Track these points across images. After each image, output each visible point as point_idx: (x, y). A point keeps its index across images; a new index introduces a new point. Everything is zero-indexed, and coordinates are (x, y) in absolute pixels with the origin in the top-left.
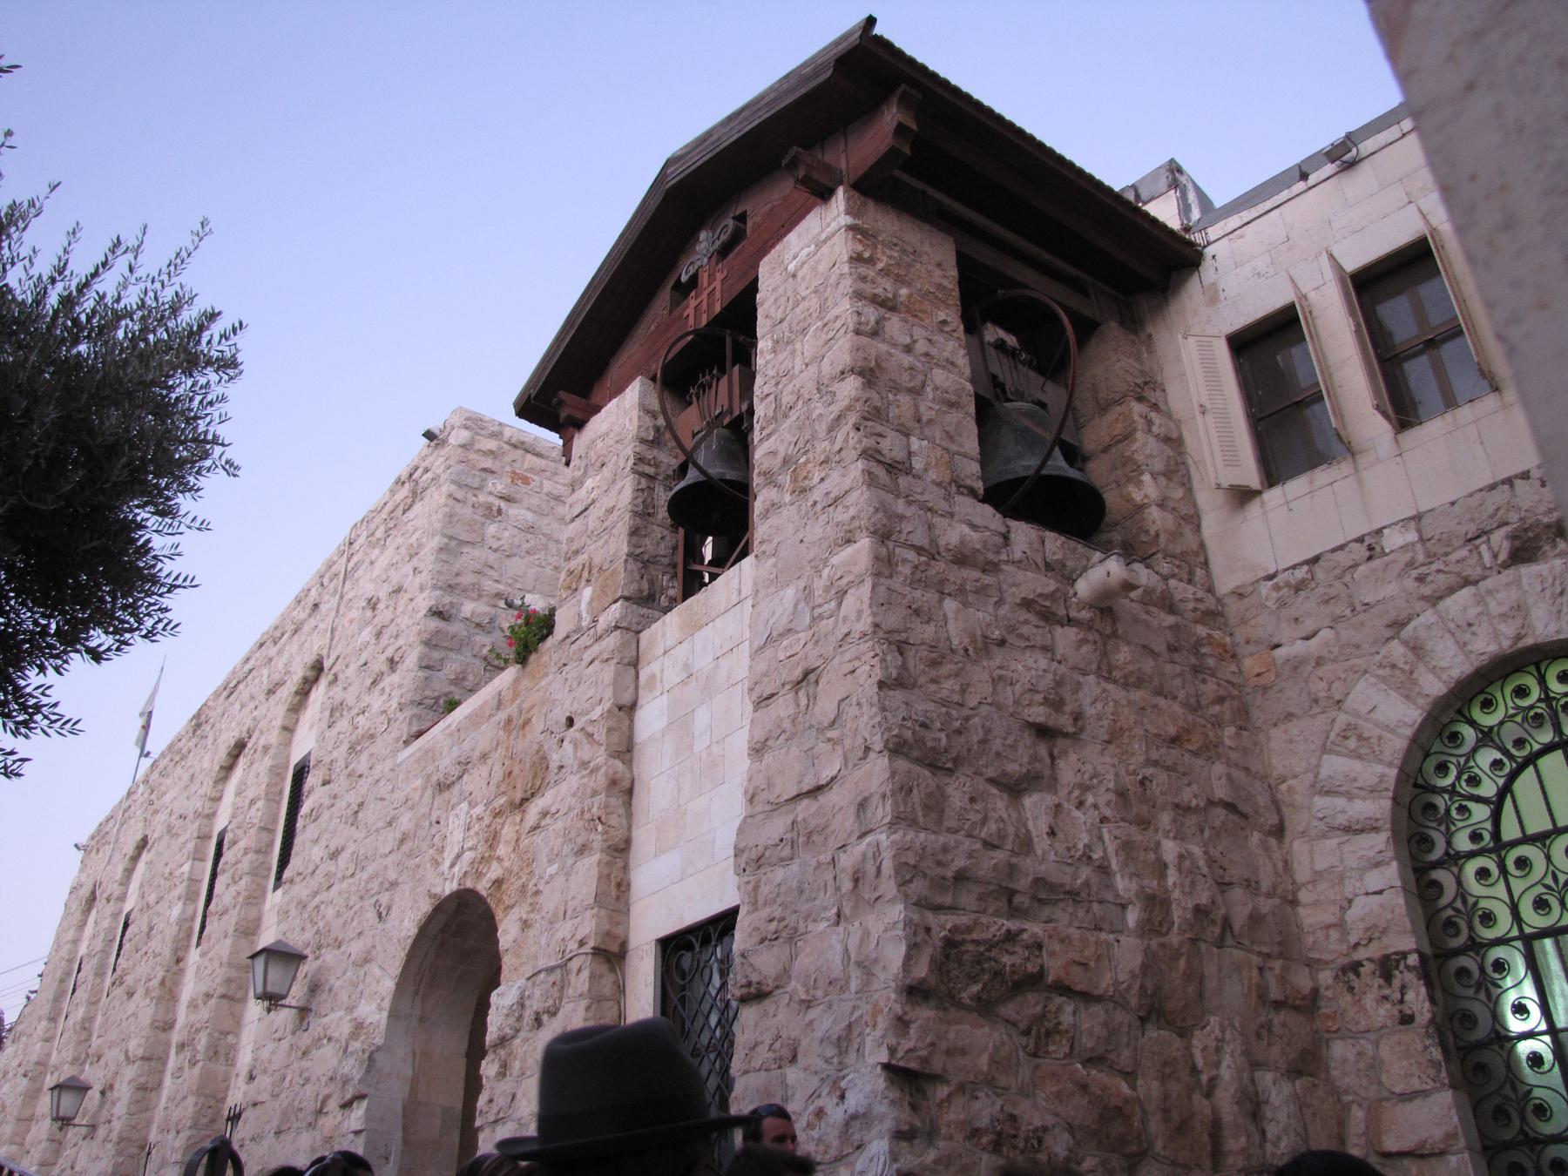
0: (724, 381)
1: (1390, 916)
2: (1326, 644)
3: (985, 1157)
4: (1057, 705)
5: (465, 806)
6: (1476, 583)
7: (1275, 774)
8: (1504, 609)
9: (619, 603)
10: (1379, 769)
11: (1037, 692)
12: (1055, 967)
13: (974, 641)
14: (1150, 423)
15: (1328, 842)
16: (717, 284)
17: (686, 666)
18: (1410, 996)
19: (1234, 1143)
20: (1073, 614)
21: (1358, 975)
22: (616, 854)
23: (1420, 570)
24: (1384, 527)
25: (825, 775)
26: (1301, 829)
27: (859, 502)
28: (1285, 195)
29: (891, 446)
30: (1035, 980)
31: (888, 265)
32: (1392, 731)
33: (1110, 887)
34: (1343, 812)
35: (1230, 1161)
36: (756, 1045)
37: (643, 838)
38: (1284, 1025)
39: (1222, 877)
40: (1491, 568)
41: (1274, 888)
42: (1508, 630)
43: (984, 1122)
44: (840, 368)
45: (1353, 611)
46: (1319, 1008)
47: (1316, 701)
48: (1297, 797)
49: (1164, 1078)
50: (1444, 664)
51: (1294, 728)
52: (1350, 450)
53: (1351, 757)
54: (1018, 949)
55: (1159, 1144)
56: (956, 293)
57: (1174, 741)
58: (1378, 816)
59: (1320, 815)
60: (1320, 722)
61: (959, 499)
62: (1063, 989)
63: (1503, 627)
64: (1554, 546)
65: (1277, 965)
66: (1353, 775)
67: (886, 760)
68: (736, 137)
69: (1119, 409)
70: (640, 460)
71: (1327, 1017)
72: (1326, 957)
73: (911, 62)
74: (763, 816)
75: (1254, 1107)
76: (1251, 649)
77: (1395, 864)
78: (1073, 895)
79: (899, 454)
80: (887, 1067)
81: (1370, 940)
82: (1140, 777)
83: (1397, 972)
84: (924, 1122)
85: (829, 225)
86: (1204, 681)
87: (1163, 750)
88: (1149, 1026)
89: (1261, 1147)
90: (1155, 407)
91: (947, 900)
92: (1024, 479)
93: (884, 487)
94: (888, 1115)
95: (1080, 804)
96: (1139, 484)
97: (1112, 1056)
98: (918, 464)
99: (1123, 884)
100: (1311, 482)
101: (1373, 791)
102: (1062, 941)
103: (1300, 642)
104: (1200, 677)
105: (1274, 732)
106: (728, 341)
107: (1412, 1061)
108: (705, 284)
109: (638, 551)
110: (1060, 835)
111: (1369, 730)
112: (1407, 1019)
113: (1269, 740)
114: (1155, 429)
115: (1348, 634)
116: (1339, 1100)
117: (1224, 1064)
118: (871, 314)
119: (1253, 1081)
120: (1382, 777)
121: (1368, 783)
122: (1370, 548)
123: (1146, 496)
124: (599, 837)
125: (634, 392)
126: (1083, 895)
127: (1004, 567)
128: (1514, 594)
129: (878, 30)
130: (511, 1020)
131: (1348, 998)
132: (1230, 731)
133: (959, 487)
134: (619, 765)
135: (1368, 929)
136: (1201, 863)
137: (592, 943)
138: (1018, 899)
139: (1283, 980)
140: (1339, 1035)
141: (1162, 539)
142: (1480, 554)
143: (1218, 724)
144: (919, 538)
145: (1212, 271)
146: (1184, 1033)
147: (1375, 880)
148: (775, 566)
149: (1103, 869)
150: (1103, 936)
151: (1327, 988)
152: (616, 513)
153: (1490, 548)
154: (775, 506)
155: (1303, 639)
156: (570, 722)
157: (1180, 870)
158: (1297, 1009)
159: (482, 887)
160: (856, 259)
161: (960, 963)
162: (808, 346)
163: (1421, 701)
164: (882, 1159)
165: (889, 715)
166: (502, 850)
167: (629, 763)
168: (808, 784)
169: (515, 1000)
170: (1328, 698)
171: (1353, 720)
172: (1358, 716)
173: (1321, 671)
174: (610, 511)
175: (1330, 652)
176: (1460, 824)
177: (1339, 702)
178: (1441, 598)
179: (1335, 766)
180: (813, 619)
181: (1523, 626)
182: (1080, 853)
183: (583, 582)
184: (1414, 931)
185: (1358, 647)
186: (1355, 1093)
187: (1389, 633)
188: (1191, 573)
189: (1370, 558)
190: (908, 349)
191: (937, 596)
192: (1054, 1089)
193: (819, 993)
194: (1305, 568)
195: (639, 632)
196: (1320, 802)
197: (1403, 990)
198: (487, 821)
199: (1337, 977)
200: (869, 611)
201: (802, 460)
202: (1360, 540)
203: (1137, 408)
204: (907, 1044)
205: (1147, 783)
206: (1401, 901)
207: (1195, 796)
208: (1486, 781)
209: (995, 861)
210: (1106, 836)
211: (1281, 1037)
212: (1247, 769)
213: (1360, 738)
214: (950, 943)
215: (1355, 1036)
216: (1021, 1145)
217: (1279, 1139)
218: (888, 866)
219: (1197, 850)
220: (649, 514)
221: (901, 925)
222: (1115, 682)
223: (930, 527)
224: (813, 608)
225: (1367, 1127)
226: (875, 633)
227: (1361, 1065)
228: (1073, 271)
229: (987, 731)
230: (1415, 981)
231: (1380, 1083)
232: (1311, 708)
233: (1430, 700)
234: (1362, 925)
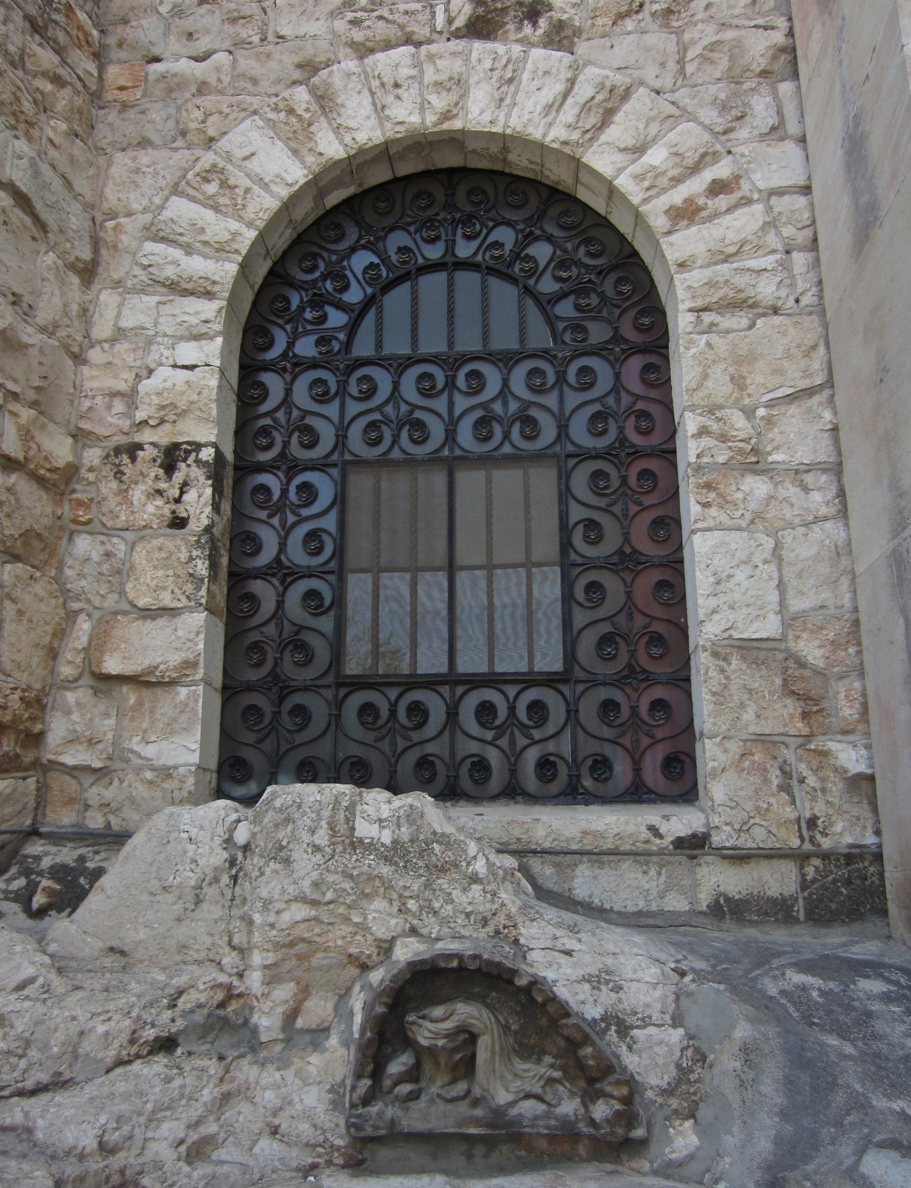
1: (195, 397)
2: (218, 69)
6: (418, 44)
7: (105, 206)
8: (442, 77)
10: (235, 225)
15: (145, 298)
18: (190, 496)
21: (133, 459)
23: (359, 14)
26: (116, 276)
32: (265, 186)
34: (176, 263)
40: (440, 33)
41: (56, 326)
42: (439, 102)
45: (262, 40)
46: (74, 491)
48: (123, 237)
50: (351, 124)
51: (145, 158)
53: (205, 206)
59: (145, 262)
60: (182, 157)
63: (433, 98)
64: (519, 29)
66: (201, 224)
71: (80, 503)
72: (101, 431)
76: (123, 55)
77: (219, 340)
81: (162, 422)
83: (182, 465)
101: (220, 250)
103: (184, 61)
105: (119, 157)
107: (170, 572)
111: (238, 178)
112: (178, 523)
113: (110, 164)
115: (247, 63)
116: (64, 604)
120: (235, 235)
121: (216, 238)
128: (457, 65)
131: (114, 485)
135: (163, 407)
139: (26, 435)
140: (87, 528)
142: (433, 14)
147: (188, 352)
151: (91, 470)
153: (447, 10)
155: (189, 57)
158: (41, 481)
163: (310, 159)
170: (200, 131)
171: (221, 164)
173: (199, 101)
175: (219, 81)
177: (212, 140)
178: (372, 51)
181: (456, 104)
184: (219, 422)
185: (255, 81)
186: (88, 601)
187: (297, 75)
196: (149, 246)
197: (184, 487)
208: (354, 287)
213: (224, 184)
215: (108, 532)
225: (90, 643)
227: (105, 568)
230: (202, 479)
231: (122, 593)
233: (323, 160)
234: (156, 400)
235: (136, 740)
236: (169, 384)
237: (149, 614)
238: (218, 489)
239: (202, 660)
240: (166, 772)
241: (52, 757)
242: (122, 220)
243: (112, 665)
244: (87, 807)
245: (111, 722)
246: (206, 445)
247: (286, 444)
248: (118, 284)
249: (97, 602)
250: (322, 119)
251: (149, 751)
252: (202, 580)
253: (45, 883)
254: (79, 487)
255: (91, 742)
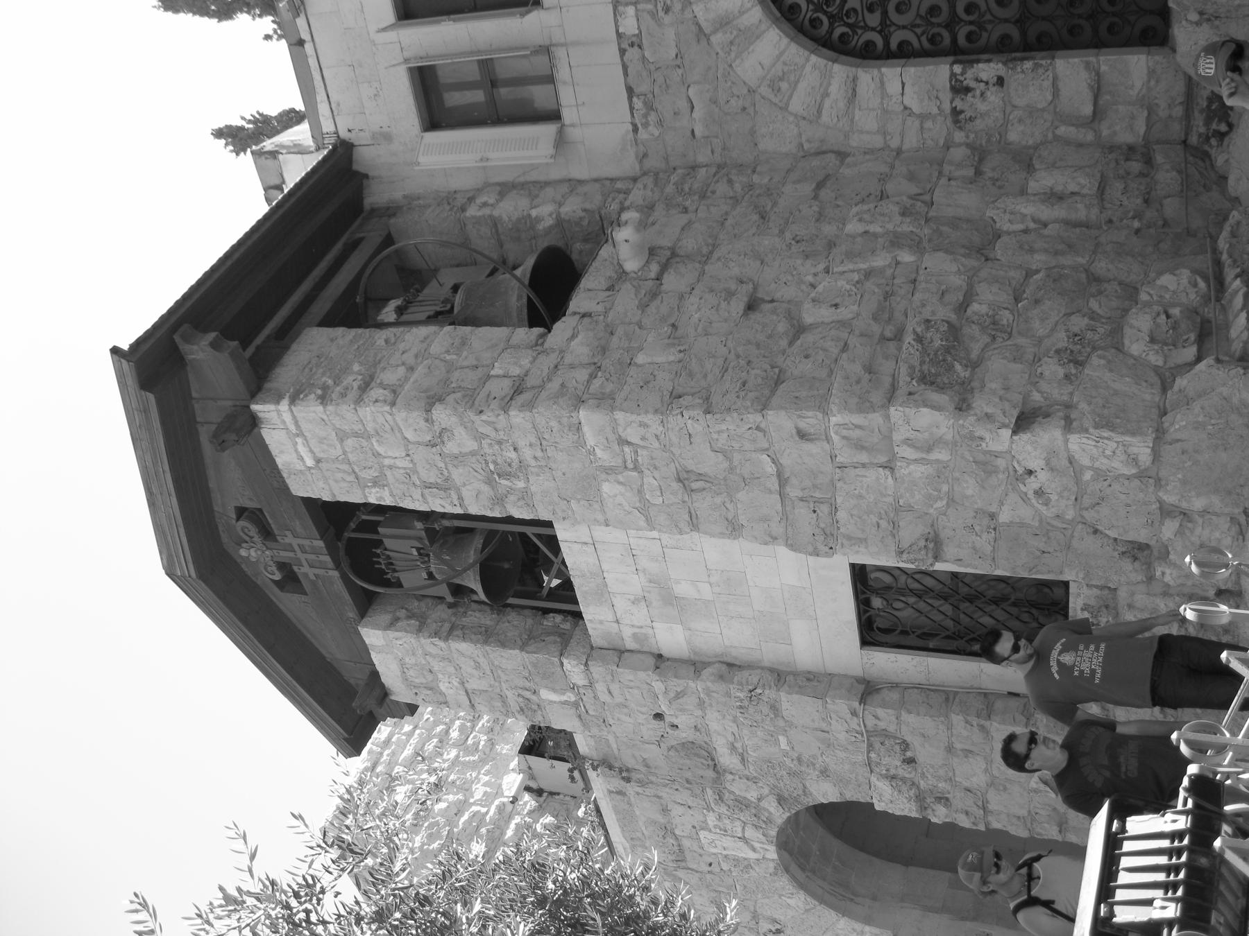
0: (388, 543)
3: (1086, 371)
4: (730, 294)
5: (702, 834)
9: (565, 661)
10: (808, 68)
11: (719, 305)
12: (944, 313)
13: (673, 345)
14: (485, 204)
15: (857, 118)
16: (295, 542)
17: (635, 602)
18: (984, 76)
19: (1081, 213)
20: (653, 275)
21: (962, 112)
22: (783, 680)
23: (660, 9)
24: (617, 31)
25: (770, 469)
27: (547, 416)
28: (312, 62)
29: (500, 387)
30: (954, 332)
31: (329, 377)
32: (782, 54)
33: (881, 271)
35: (1093, 217)
36: (974, 548)
37: (771, 653)
38: (993, 169)
39: (876, 196)
43: (1061, 372)
44: (422, 423)
45: (679, 67)
46: (981, 145)
47: (744, 109)
49: (1032, 251)
52: (546, 50)
54: (929, 335)
55: (1080, 260)
56: (360, 331)
57: (763, 217)
58: (845, 75)
61: (546, 345)
62: (962, 307)
65: (947, 168)
67: (770, 412)
68: (174, 500)
69: (469, 227)
70: (436, 634)
71: (989, 141)
72: (944, 133)
73: (156, 327)
74: (789, 529)
75: (1054, 197)
77: (884, 70)
78: (887, 296)
79: (507, 383)
80: (1015, 432)
81: (937, 98)
82: (793, 242)
83: (965, 83)
84: (1059, 410)
85: (284, 422)
86: (713, 192)
87: (771, 225)
88: (992, 256)
89: (1084, 196)
90: (471, 200)
91: (887, 380)
92: (529, 299)
93: (536, 397)
94: (1048, 435)
95: (813, 286)
96: (538, 219)
97: (1014, 283)
98: (516, 371)
99: (880, 261)
100: (565, 83)
102: (924, 305)
103: (694, 115)
104: (709, 194)
105: (761, 146)
106: (353, 535)
108: (291, 554)
109: (520, 643)
110: (837, 300)
112: (1000, 81)
114: (491, 201)
117: (1024, 211)
118: (376, 393)
119: (1035, 195)
120: (814, 67)
122: (632, 45)
123: (550, 215)
124: (767, 692)
125: (372, 636)
126: (888, 288)
127: (609, 319)
129: (125, 347)
130: (904, 788)
131: (978, 122)
132: (756, 178)
133: (536, 345)
134: (706, 672)
135: (929, 98)
136: (865, 207)
137: (856, 704)
138: (888, 334)
141: (588, 206)
143: (751, 187)
144: (582, 375)
145: (362, 134)
146: (998, 236)
147: (894, 87)
148: (579, 501)
149: (868, 274)
150: (921, 278)
151: (967, 137)
152: (482, 660)
154: (525, 496)
156: (659, 716)
157: (871, 223)
158: (981, 160)
159: (780, 816)
160: (323, 399)
161: (937, 375)
162: (392, 452)
163: (763, 27)
164: (1085, 440)
165: (733, 407)
166: (752, 795)
167: (706, 665)
168: (773, 484)
169: (887, 783)
172: (764, 78)
174: (478, 666)
175: (708, 91)
176: (860, 18)
179: (796, 105)
180: (636, 468)
182: (853, 288)
183: (534, 698)
186: (1047, 129)
187: (704, 42)
188: (619, 191)
189: (640, 47)
190: (411, 369)
191: (632, 368)
192: (1038, 323)
193: (945, 488)
194: (635, 99)
195: (592, 648)
196: (825, 118)
197: (978, 80)
198: (723, 809)
199: (960, 128)
200: (643, 416)
201: (492, 467)
202: (622, 52)
203: (472, 211)
204: (1001, 418)
205: (798, 238)
206: (912, 70)
207: (811, 207)
209: (858, 345)
210: (841, 269)
211: (1003, 173)
212: (789, 171)
213: (781, 79)
214: (923, 379)
216: (1078, 347)
217: (1079, 184)
218: (857, 419)
219: (855, 210)
220: (486, 631)
221: (907, 410)
222: (711, 252)
223: (572, 367)
224: (626, 467)
225: (1073, 125)
226: (662, 414)
228: (339, 246)
229: (749, 342)
230: (973, 70)
231: (1043, 110)
232: (748, 114)
235: (1131, 92)
236: (915, 96)
237: (1056, 92)
238: (978, 61)
239: (1085, 59)
240: (1151, 73)
241: (1141, 140)
242: (804, 138)
243: (1088, 110)
244: (1170, 116)
245: (1121, 108)
246: (952, 70)
247: (939, 25)
248: (846, 136)
249: (1048, 124)
250: (735, 23)
251: (1138, 84)
252: (1036, 64)
253: (1214, 126)
254: (978, 142)
255: (1133, 117)
